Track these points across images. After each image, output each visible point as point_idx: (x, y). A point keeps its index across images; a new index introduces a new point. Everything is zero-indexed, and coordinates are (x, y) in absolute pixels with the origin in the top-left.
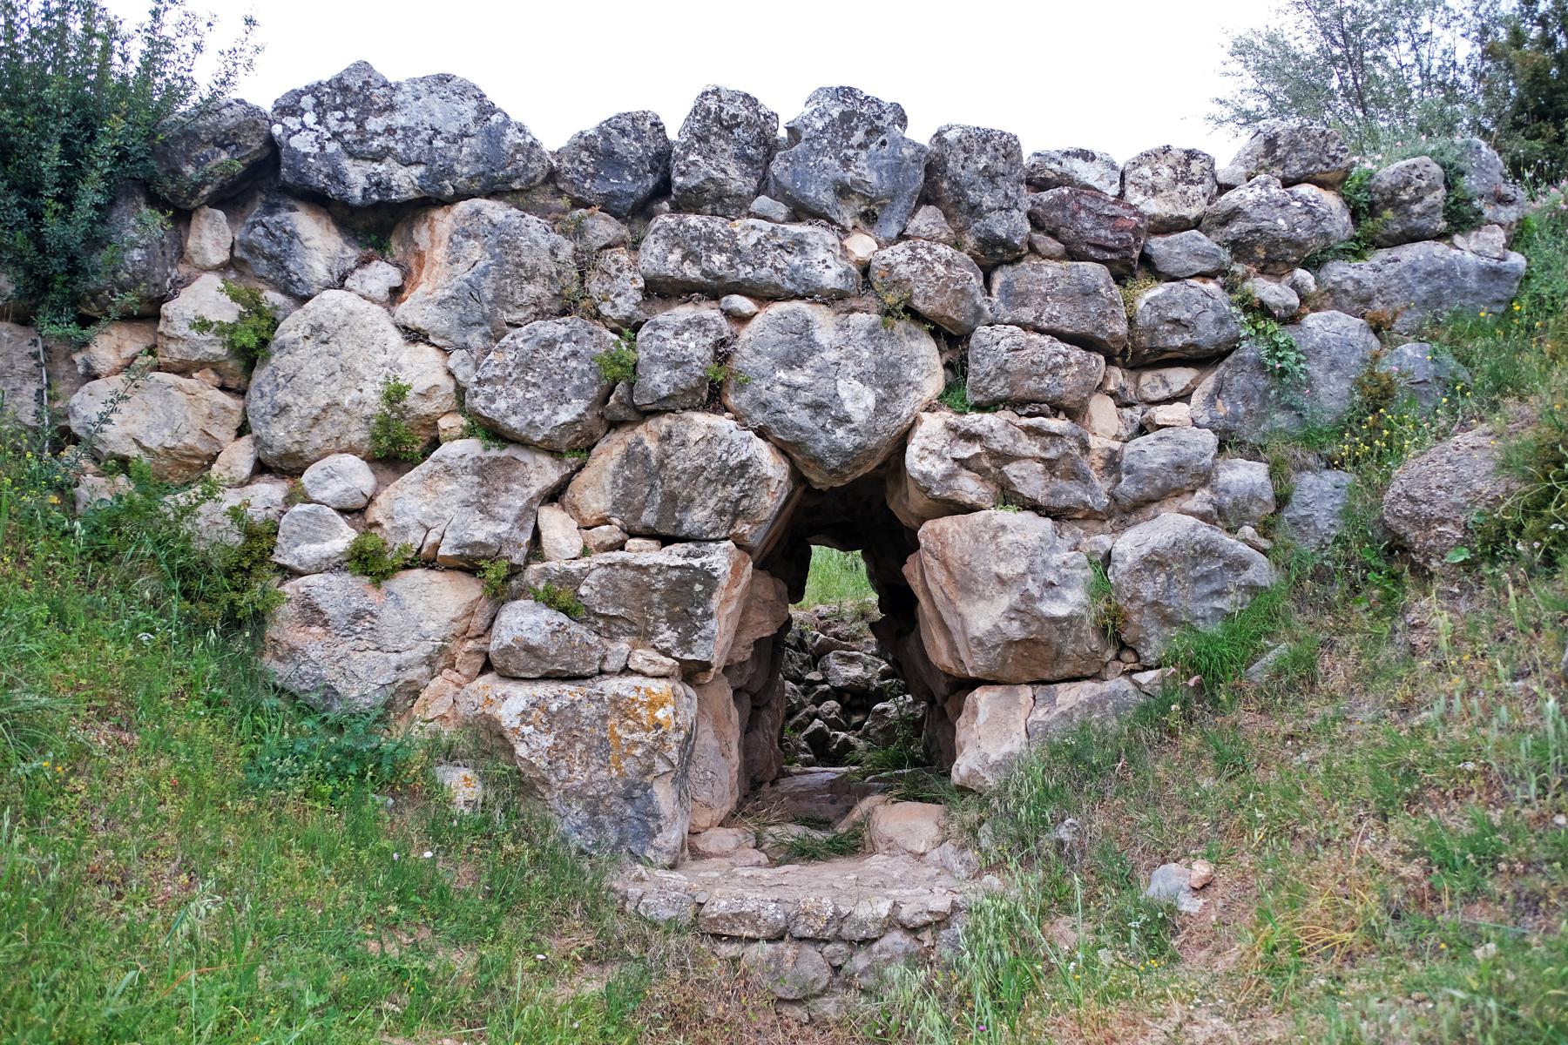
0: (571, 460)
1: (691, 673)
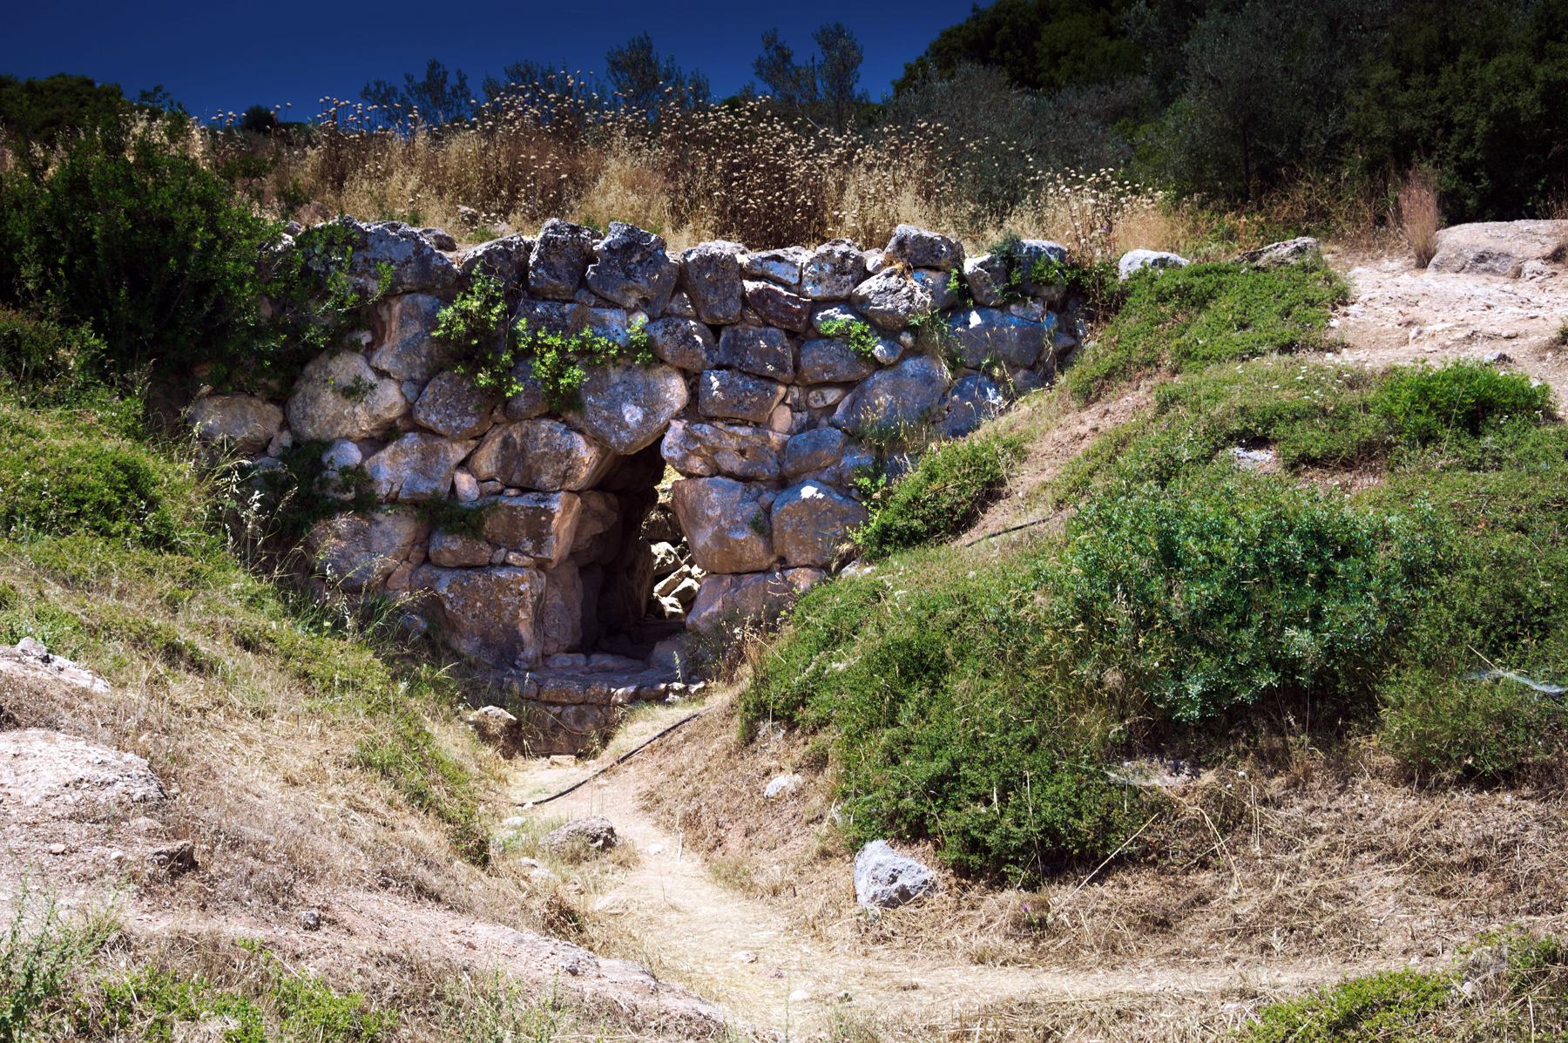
0: (472, 443)
1: (541, 565)
